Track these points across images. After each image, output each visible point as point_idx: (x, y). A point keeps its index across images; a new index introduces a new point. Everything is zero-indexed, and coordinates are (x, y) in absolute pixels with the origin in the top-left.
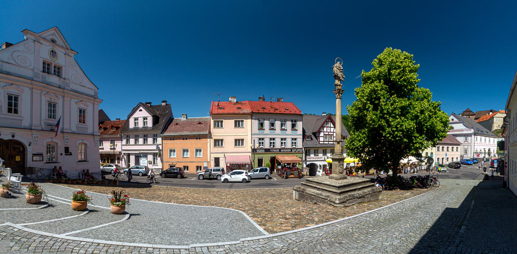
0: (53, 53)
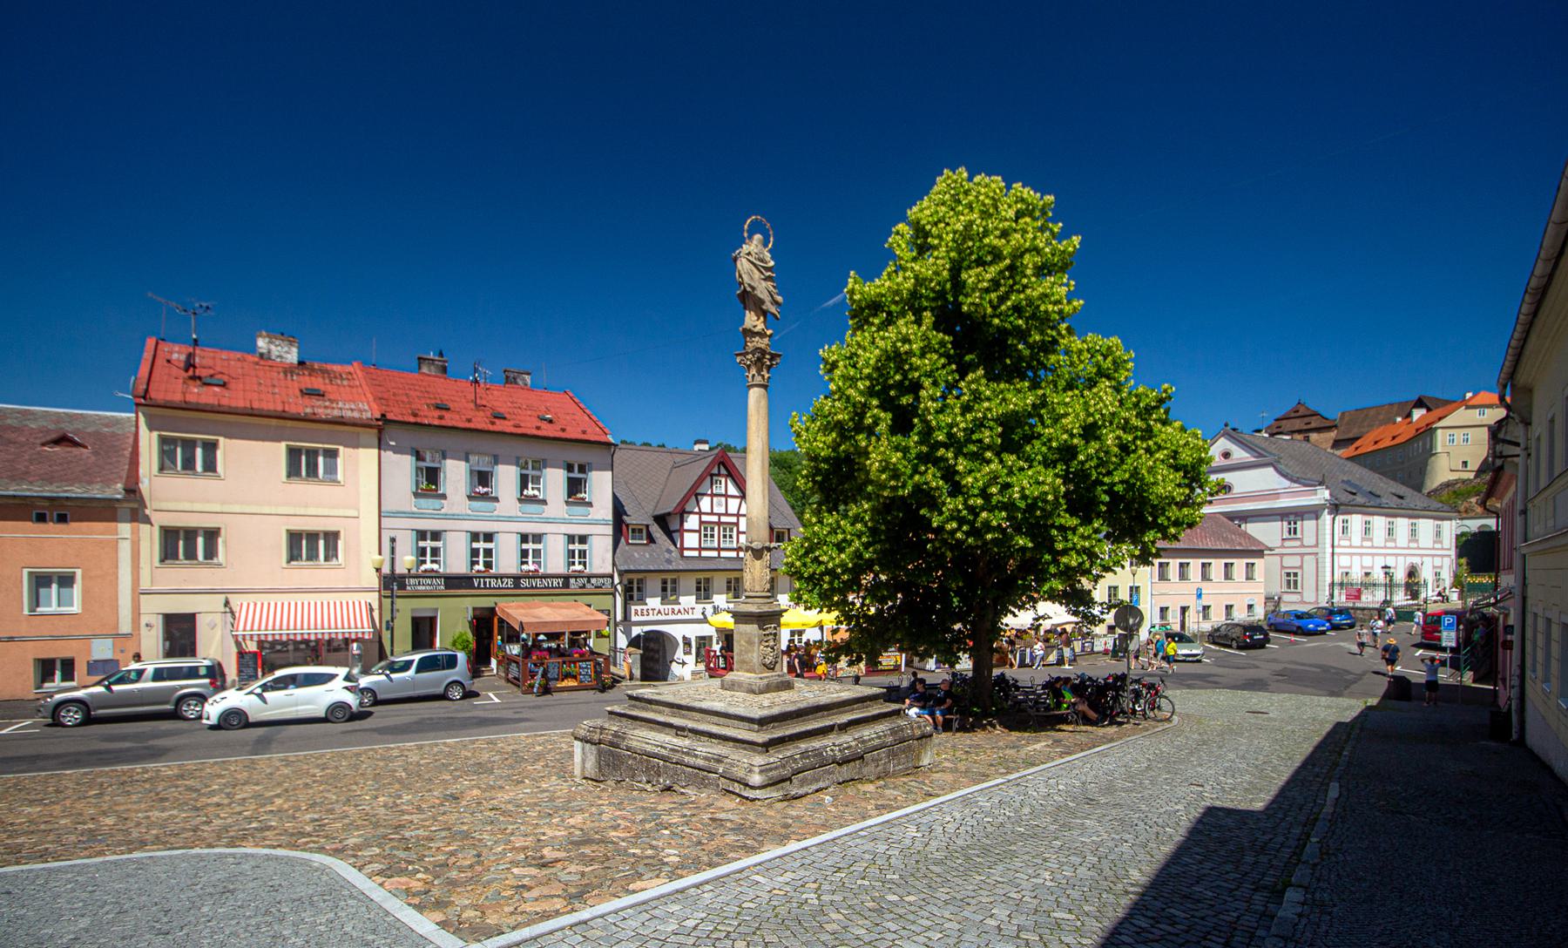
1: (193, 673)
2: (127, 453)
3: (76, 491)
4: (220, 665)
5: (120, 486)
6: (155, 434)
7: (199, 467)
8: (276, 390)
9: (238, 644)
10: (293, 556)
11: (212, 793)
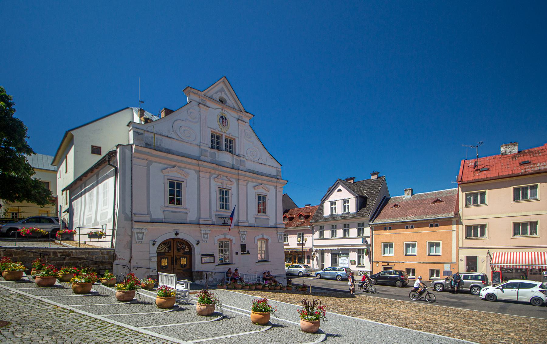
1: (476, 278)
2: (455, 202)
3: (441, 216)
4: (486, 275)
5: (453, 213)
6: (464, 193)
7: (479, 203)
8: (509, 166)
9: (492, 268)
10: (516, 233)
11: (485, 324)
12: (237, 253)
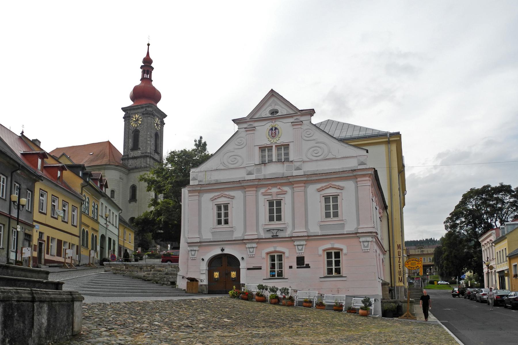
0: (274, 131)
12: (292, 268)
